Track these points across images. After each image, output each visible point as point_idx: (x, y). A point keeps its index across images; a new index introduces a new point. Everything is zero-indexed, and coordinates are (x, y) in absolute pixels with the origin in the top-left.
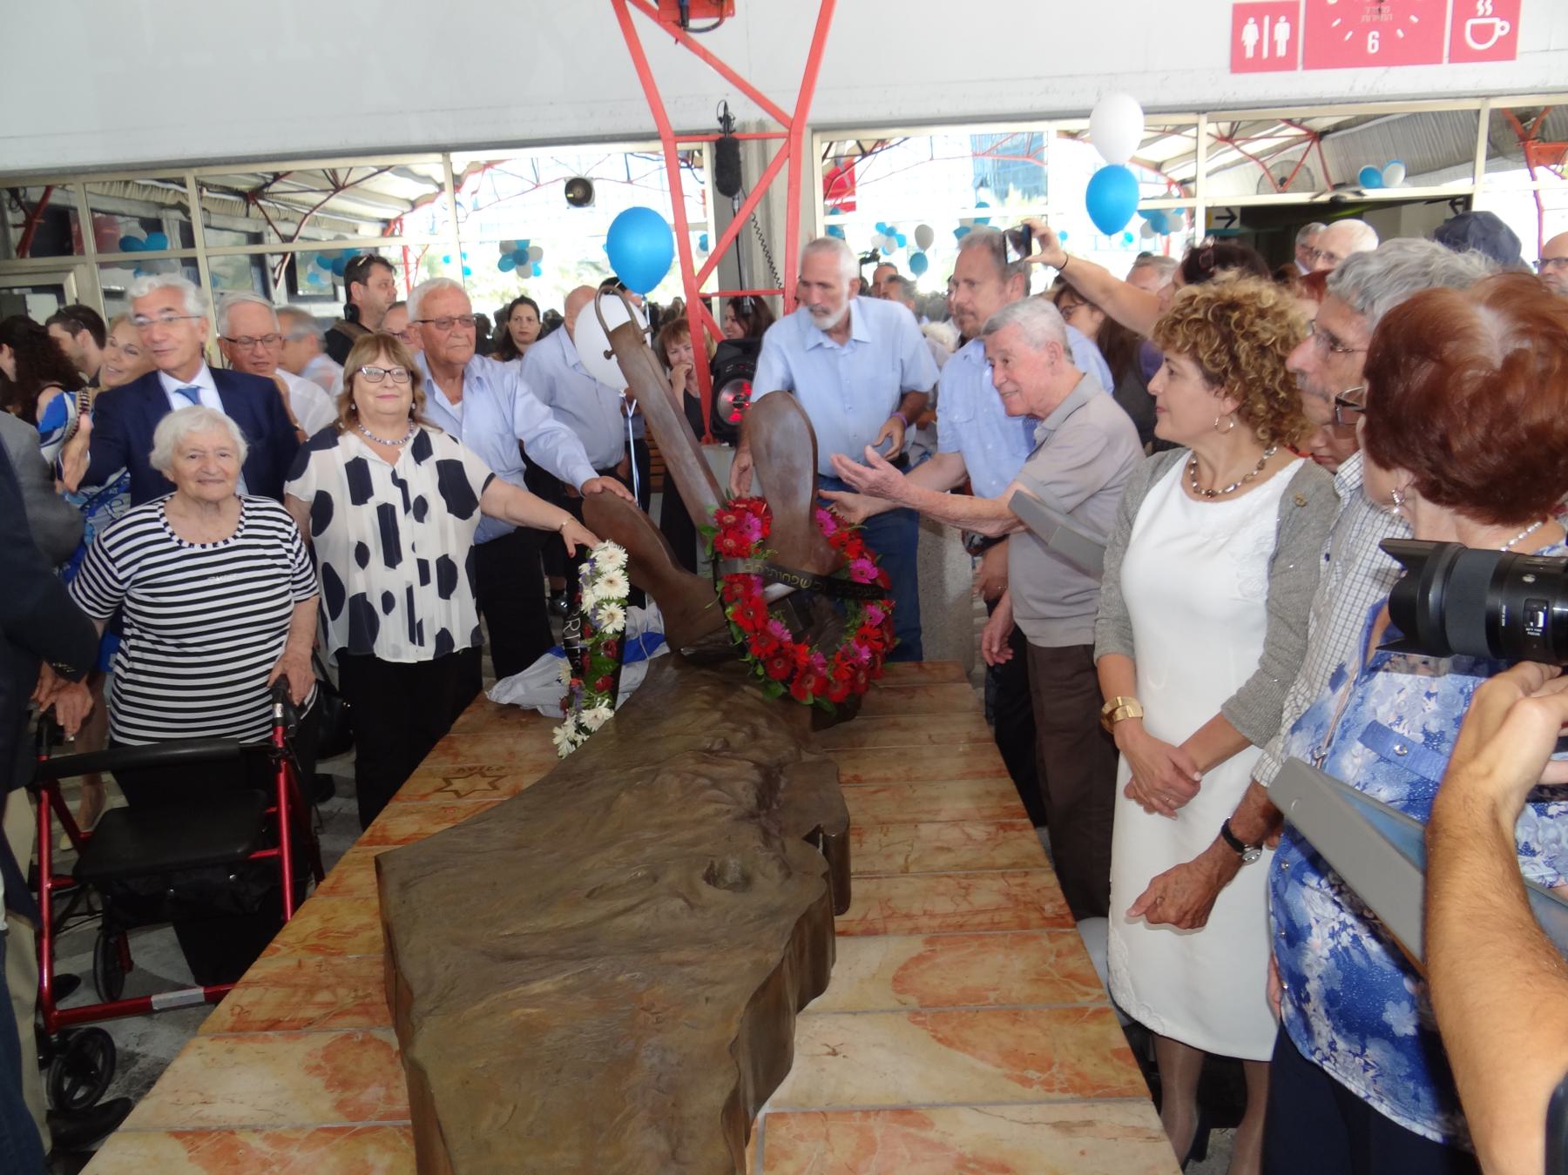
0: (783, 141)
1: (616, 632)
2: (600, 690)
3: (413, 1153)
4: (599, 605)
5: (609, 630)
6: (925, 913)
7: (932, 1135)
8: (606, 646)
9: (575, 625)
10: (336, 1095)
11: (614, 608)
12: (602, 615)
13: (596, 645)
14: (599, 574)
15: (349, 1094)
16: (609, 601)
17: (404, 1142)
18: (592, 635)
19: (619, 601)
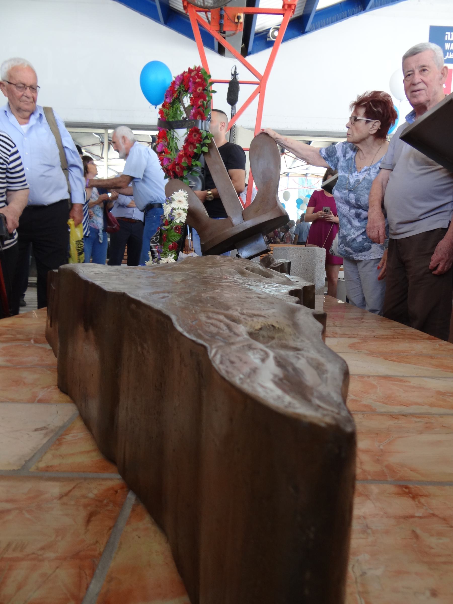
0: (257, 86)
1: (181, 222)
2: (171, 249)
3: (56, 375)
4: (173, 209)
5: (178, 221)
6: (353, 334)
7: (411, 384)
8: (176, 228)
9: (156, 239)
10: (8, 358)
11: (181, 211)
12: (175, 213)
13: (172, 228)
14: (173, 199)
15: (14, 358)
16: (178, 209)
17: (49, 372)
18: (168, 225)
19: (184, 210)
